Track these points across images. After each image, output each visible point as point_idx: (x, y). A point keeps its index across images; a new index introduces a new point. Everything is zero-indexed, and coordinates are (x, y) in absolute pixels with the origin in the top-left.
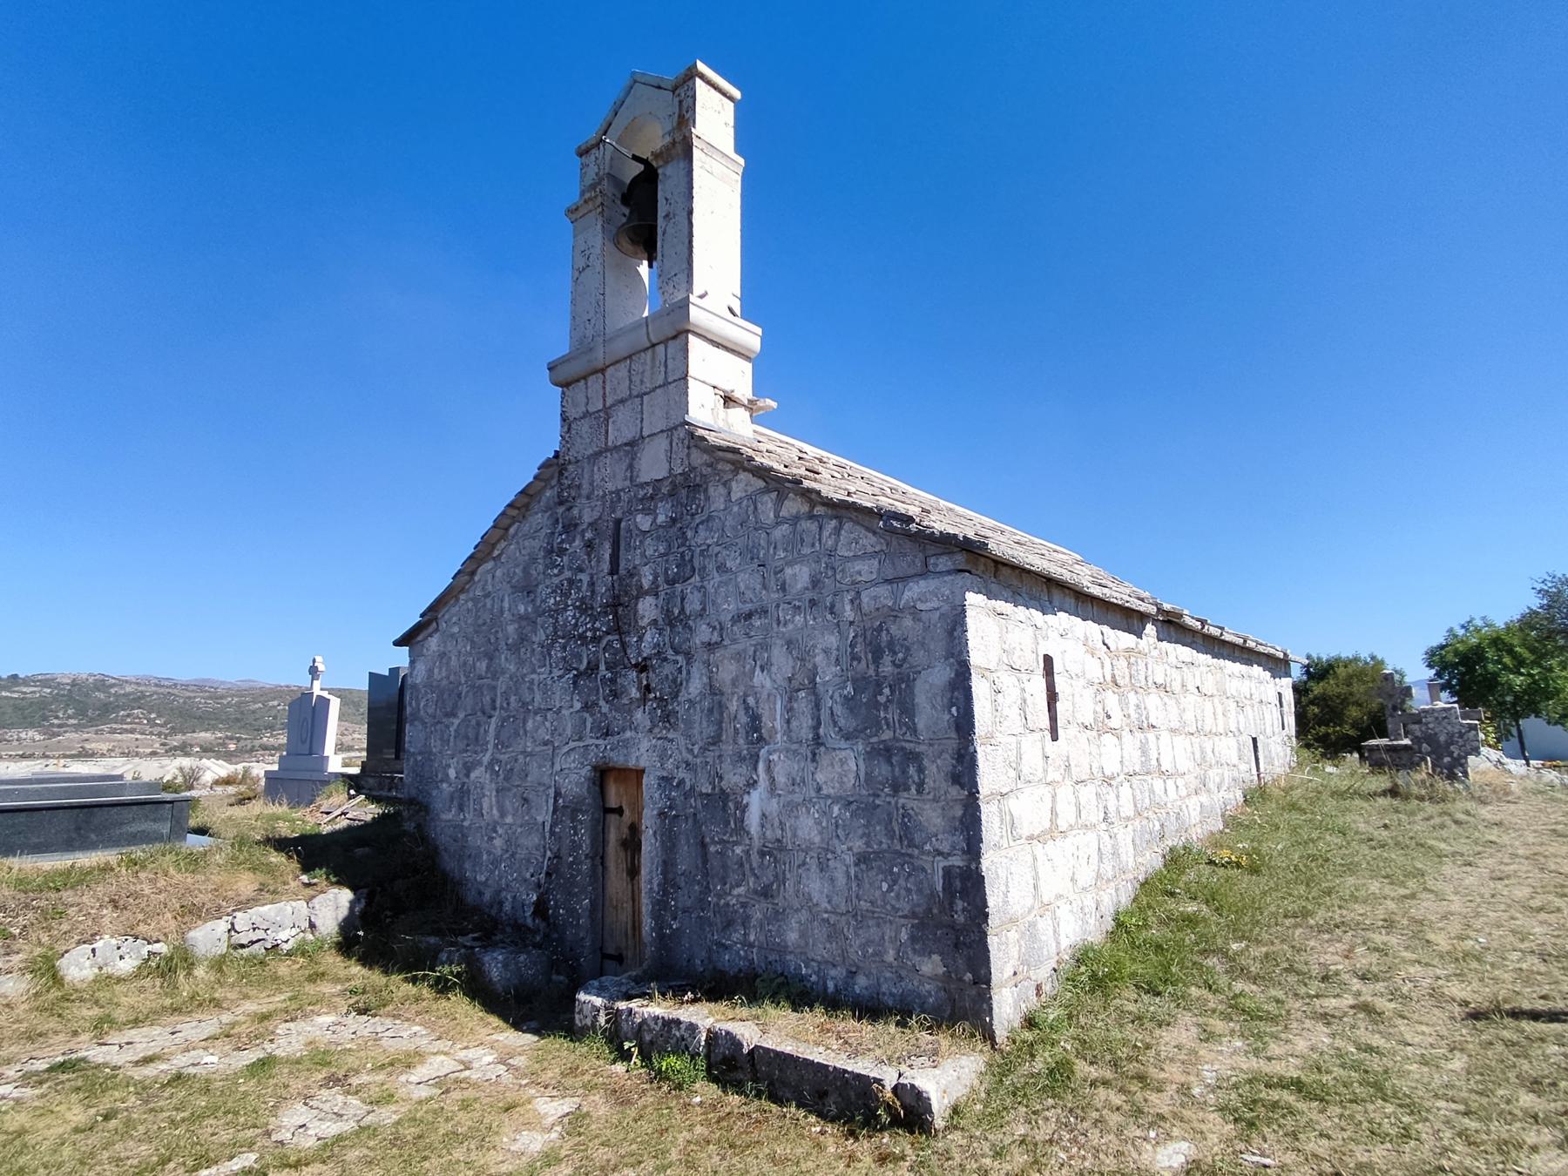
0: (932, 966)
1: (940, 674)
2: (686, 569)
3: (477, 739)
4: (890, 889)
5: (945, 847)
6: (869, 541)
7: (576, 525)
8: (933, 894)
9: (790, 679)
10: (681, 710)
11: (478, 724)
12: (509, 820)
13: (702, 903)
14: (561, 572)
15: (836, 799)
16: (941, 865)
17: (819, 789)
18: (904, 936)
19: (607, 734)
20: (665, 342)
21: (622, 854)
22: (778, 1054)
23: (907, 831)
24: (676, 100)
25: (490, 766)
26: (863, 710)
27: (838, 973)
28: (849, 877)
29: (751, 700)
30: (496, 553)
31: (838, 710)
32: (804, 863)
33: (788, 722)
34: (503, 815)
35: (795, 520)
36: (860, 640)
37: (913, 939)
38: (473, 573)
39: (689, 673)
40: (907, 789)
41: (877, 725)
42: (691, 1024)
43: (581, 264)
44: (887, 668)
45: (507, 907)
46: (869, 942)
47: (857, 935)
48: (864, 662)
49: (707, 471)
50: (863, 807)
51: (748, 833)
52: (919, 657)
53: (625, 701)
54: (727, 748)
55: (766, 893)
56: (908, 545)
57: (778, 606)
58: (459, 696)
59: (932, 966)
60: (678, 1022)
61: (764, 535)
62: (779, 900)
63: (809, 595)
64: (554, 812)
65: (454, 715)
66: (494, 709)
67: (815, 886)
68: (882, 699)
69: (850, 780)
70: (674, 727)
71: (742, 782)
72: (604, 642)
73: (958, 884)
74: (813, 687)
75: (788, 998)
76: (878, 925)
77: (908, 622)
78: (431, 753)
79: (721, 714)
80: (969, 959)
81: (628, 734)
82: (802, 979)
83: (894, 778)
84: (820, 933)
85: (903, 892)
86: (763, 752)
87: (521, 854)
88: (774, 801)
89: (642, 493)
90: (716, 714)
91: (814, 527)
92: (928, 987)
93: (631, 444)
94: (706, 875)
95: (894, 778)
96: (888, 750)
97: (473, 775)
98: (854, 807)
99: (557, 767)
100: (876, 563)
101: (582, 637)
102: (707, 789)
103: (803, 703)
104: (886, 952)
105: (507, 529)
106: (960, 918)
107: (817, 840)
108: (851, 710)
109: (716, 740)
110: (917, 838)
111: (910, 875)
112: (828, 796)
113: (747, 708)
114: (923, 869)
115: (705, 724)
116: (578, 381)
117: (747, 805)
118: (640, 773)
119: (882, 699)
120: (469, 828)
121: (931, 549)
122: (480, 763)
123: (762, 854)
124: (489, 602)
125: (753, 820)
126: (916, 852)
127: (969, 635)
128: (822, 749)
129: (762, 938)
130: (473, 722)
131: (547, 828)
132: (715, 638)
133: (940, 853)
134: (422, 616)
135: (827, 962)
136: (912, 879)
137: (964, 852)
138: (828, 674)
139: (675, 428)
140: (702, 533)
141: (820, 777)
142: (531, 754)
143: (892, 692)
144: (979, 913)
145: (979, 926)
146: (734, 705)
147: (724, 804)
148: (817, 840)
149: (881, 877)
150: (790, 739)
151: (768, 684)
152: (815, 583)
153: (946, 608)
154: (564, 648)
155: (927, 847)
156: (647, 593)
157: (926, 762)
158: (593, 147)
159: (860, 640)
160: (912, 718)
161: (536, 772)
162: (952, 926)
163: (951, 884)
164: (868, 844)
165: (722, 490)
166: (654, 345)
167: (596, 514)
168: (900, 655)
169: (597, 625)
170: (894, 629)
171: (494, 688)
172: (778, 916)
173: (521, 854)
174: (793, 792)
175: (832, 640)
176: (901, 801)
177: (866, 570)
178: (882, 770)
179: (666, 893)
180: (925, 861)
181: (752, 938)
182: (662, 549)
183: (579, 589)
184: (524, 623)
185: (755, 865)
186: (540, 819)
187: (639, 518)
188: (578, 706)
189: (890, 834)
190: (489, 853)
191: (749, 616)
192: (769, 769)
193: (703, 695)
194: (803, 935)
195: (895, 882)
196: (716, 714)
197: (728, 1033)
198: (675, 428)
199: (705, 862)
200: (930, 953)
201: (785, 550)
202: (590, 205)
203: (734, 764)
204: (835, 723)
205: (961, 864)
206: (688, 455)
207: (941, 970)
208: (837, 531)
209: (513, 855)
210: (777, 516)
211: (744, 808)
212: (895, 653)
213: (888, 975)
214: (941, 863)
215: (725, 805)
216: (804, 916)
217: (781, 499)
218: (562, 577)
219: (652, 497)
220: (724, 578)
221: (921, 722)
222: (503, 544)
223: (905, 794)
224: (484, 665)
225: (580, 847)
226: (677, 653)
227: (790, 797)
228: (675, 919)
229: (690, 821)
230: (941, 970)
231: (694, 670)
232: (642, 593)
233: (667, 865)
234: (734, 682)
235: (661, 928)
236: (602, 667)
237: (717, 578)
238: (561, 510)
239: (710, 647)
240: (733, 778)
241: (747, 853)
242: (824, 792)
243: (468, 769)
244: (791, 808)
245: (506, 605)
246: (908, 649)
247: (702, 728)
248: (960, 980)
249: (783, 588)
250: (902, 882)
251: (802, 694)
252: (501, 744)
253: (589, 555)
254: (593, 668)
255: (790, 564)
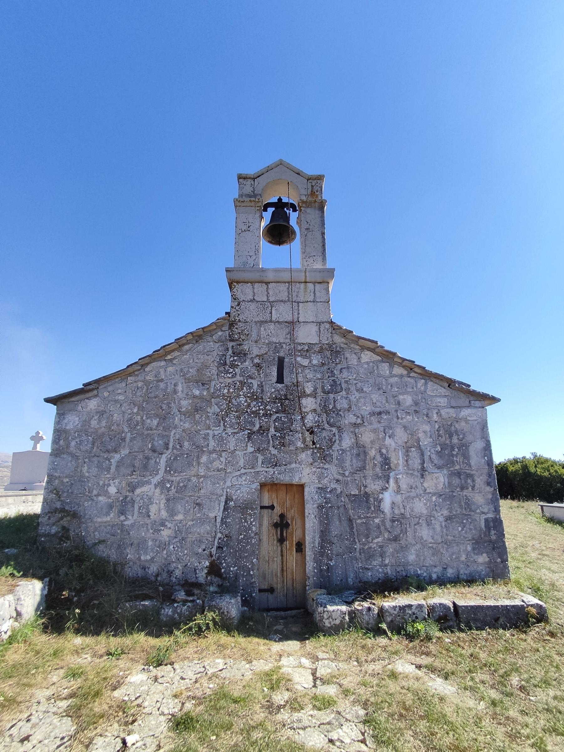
0: (483, 559)
1: (479, 445)
2: (335, 387)
3: (145, 467)
4: (462, 530)
5: (486, 510)
6: (443, 391)
7: (245, 355)
8: (481, 530)
9: (406, 443)
10: (335, 454)
11: (148, 458)
12: (180, 517)
13: (351, 550)
14: (234, 376)
15: (434, 494)
16: (484, 518)
17: (426, 490)
18: (469, 548)
19: (276, 465)
20: (314, 283)
21: (274, 531)
22: (472, 607)
23: (468, 505)
24: (310, 185)
25: (161, 484)
26: (446, 457)
27: (438, 569)
28: (441, 526)
29: (384, 451)
30: (169, 357)
31: (434, 456)
32: (418, 523)
33: (407, 461)
34: (172, 513)
35: (401, 376)
36: (442, 429)
37: (474, 549)
38: (143, 366)
39: (340, 436)
40: (467, 489)
41: (453, 463)
42: (419, 605)
43: (244, 228)
44: (455, 440)
45: (178, 573)
46: (453, 554)
47: (447, 551)
48: (444, 438)
49: (342, 346)
50: (447, 496)
51: (383, 512)
52: (469, 438)
53: (292, 448)
54: (369, 472)
55: (396, 539)
56: (462, 395)
57: (396, 411)
58: (123, 439)
59: (483, 559)
60: (410, 606)
61: (384, 380)
62: (403, 542)
63: (414, 408)
64: (225, 509)
65: (116, 451)
66: (167, 449)
67: (425, 533)
68: (454, 453)
69: (441, 486)
70: (330, 462)
71: (378, 488)
72: (274, 417)
73: (492, 524)
74: (419, 447)
75: (375, 592)
76: (457, 545)
77: (463, 424)
78: (83, 476)
79: (366, 456)
80: (499, 553)
81: (294, 465)
82: (418, 576)
83: (462, 484)
84: (428, 553)
85: (468, 530)
86: (391, 474)
87: (191, 538)
88: (399, 497)
89: (300, 348)
90: (362, 456)
91: (412, 381)
92: (481, 568)
93: (292, 323)
94: (352, 534)
95: (462, 484)
96: (459, 473)
97: (138, 491)
98: (443, 496)
99: (228, 484)
100: (446, 399)
101: (256, 413)
102: (355, 492)
103: (414, 453)
104: (461, 556)
105: (184, 345)
106: (494, 538)
107: (425, 512)
108: (440, 457)
109: (363, 468)
110: (473, 508)
111: (471, 523)
112: (430, 493)
113: (382, 454)
114: (476, 520)
115: (354, 461)
116: (247, 282)
117: (382, 499)
118: (301, 487)
119: (454, 453)
120: (132, 525)
121: (472, 398)
122: (148, 482)
123: (393, 521)
124: (162, 385)
125: (386, 506)
126: (473, 513)
127: (489, 430)
128: (427, 473)
129: (393, 561)
130: (141, 456)
131: (219, 520)
132: (359, 421)
133: (483, 513)
134: (85, 385)
135: (432, 566)
136: (472, 524)
137: (494, 512)
138: (425, 442)
139: (323, 323)
140: (345, 374)
141: (426, 485)
142: (204, 477)
143: (459, 450)
144: (501, 535)
145: (502, 539)
146: (372, 453)
147: (365, 500)
148: (425, 512)
149: (458, 525)
150: (409, 469)
151: (393, 444)
152: (416, 404)
153: (480, 420)
154: (238, 417)
155: (478, 511)
156: (308, 396)
157: (475, 478)
158: (250, 178)
159: (442, 429)
160: (469, 460)
161: (207, 487)
162: (490, 541)
163: (489, 525)
164: (450, 512)
165: (354, 356)
166: (306, 282)
167: (263, 351)
168: (461, 436)
169: (268, 407)
170: (457, 426)
171: (168, 436)
172: (404, 549)
173: (191, 538)
174: (411, 492)
175: (427, 428)
176: (464, 493)
177: (443, 402)
178: (456, 481)
179: (322, 547)
180: (477, 517)
181: (387, 562)
182: (319, 376)
183: (250, 388)
184: (196, 400)
185: (388, 527)
186: (212, 515)
187: (299, 359)
188: (250, 449)
189: (461, 506)
190: (154, 540)
191: (380, 413)
192: (397, 481)
193: (351, 448)
194: (417, 556)
195: (464, 527)
196: (362, 456)
197: (440, 604)
198: (323, 323)
199: (352, 528)
200: (482, 553)
201: (397, 388)
202: (253, 204)
203: (374, 480)
204: (432, 462)
205: (492, 516)
206: (332, 337)
207: (487, 559)
208: (426, 384)
209: (183, 539)
210: (391, 373)
211: (380, 501)
212: (458, 435)
213: (462, 566)
214: (484, 517)
215: (367, 501)
216: (418, 546)
217: (391, 367)
218: (233, 380)
219: (307, 351)
220: (362, 395)
221: (473, 462)
222: (176, 354)
223: (466, 491)
224: (155, 422)
225: (250, 529)
226: (331, 426)
227: (408, 494)
228: (331, 560)
229: (342, 509)
230: (487, 559)
231: (345, 435)
232: (304, 395)
233: (324, 534)
234: (372, 442)
235: (320, 566)
236: (272, 430)
237: (357, 395)
238: (230, 344)
239: (355, 425)
240: (373, 486)
241: (383, 521)
242: (428, 491)
243: (133, 488)
244: (409, 499)
245: (180, 388)
246: (464, 434)
247: (350, 463)
248: (496, 562)
249: (399, 403)
250: (467, 526)
251: (413, 449)
252: (170, 468)
253: (258, 371)
254: (263, 430)
255: (403, 394)
